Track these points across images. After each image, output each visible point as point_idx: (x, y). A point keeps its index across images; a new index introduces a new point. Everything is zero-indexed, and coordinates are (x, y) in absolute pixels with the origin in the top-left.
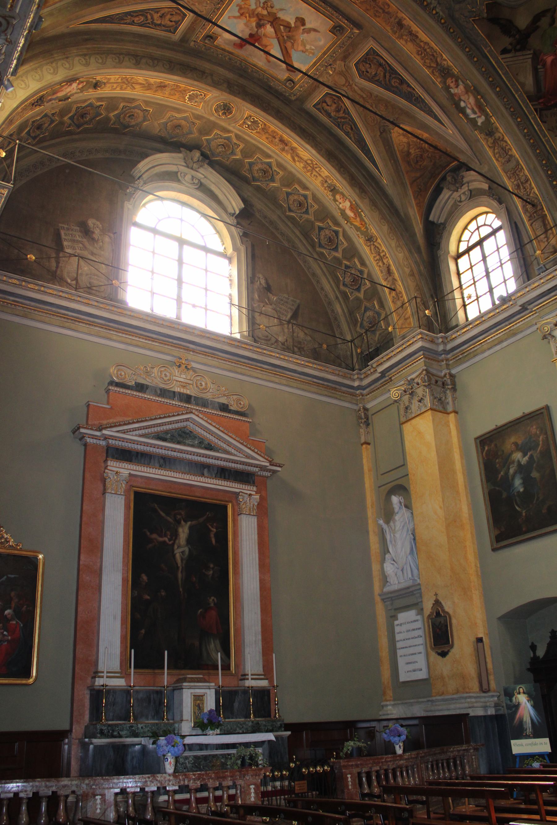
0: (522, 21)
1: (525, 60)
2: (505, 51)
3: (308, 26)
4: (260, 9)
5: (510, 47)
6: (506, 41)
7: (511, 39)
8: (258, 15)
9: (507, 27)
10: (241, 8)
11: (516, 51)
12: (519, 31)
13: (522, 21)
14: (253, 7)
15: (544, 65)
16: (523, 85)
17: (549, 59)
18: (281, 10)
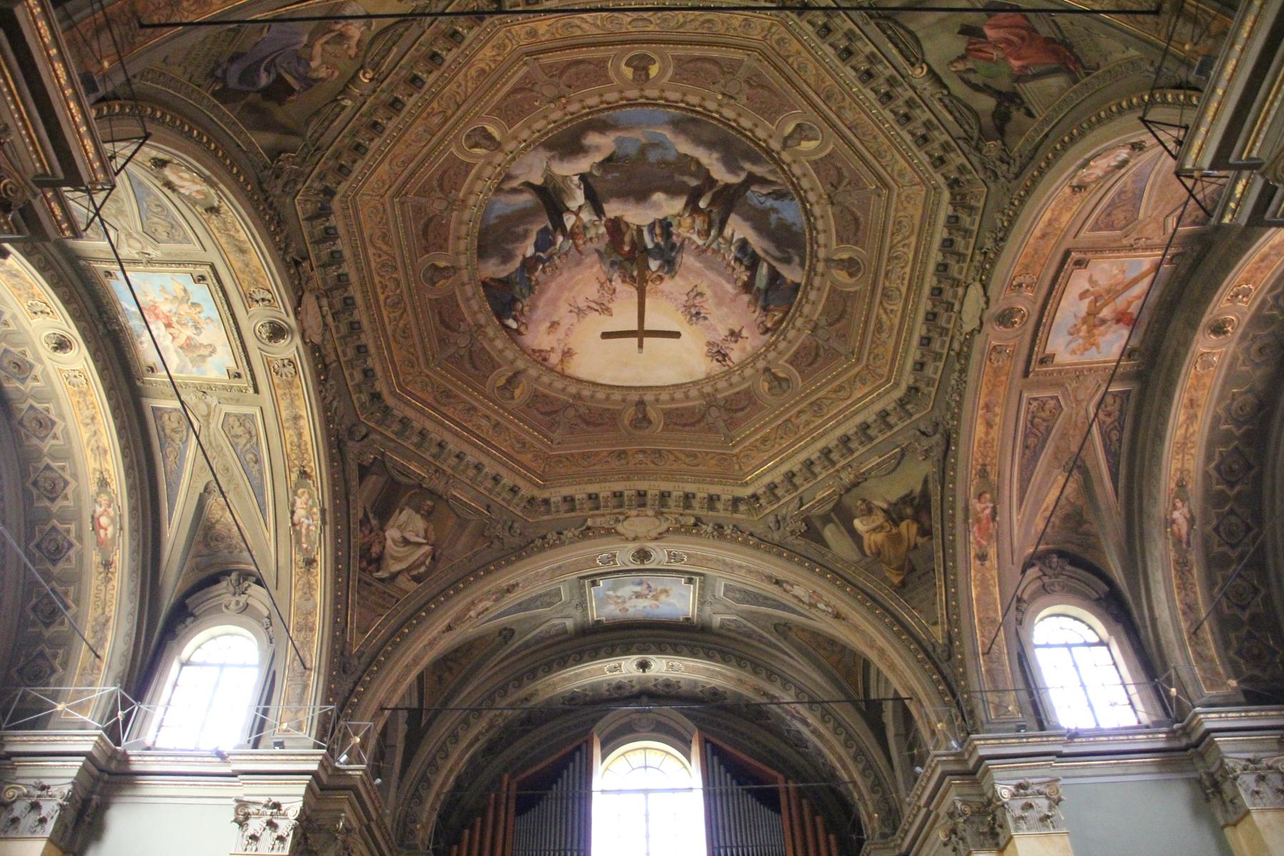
0: (986, 103)
1: (1030, 90)
2: (1030, 114)
3: (1087, 286)
4: (1082, 334)
5: (1023, 110)
6: (1017, 115)
7: (1013, 109)
8: (1089, 331)
9: (1001, 118)
10: (1086, 349)
11: (1023, 102)
12: (999, 105)
13: (986, 103)
14: (1081, 341)
15: (1025, 67)
16: (1062, 90)
17: (1016, 64)
18: (1076, 316)
